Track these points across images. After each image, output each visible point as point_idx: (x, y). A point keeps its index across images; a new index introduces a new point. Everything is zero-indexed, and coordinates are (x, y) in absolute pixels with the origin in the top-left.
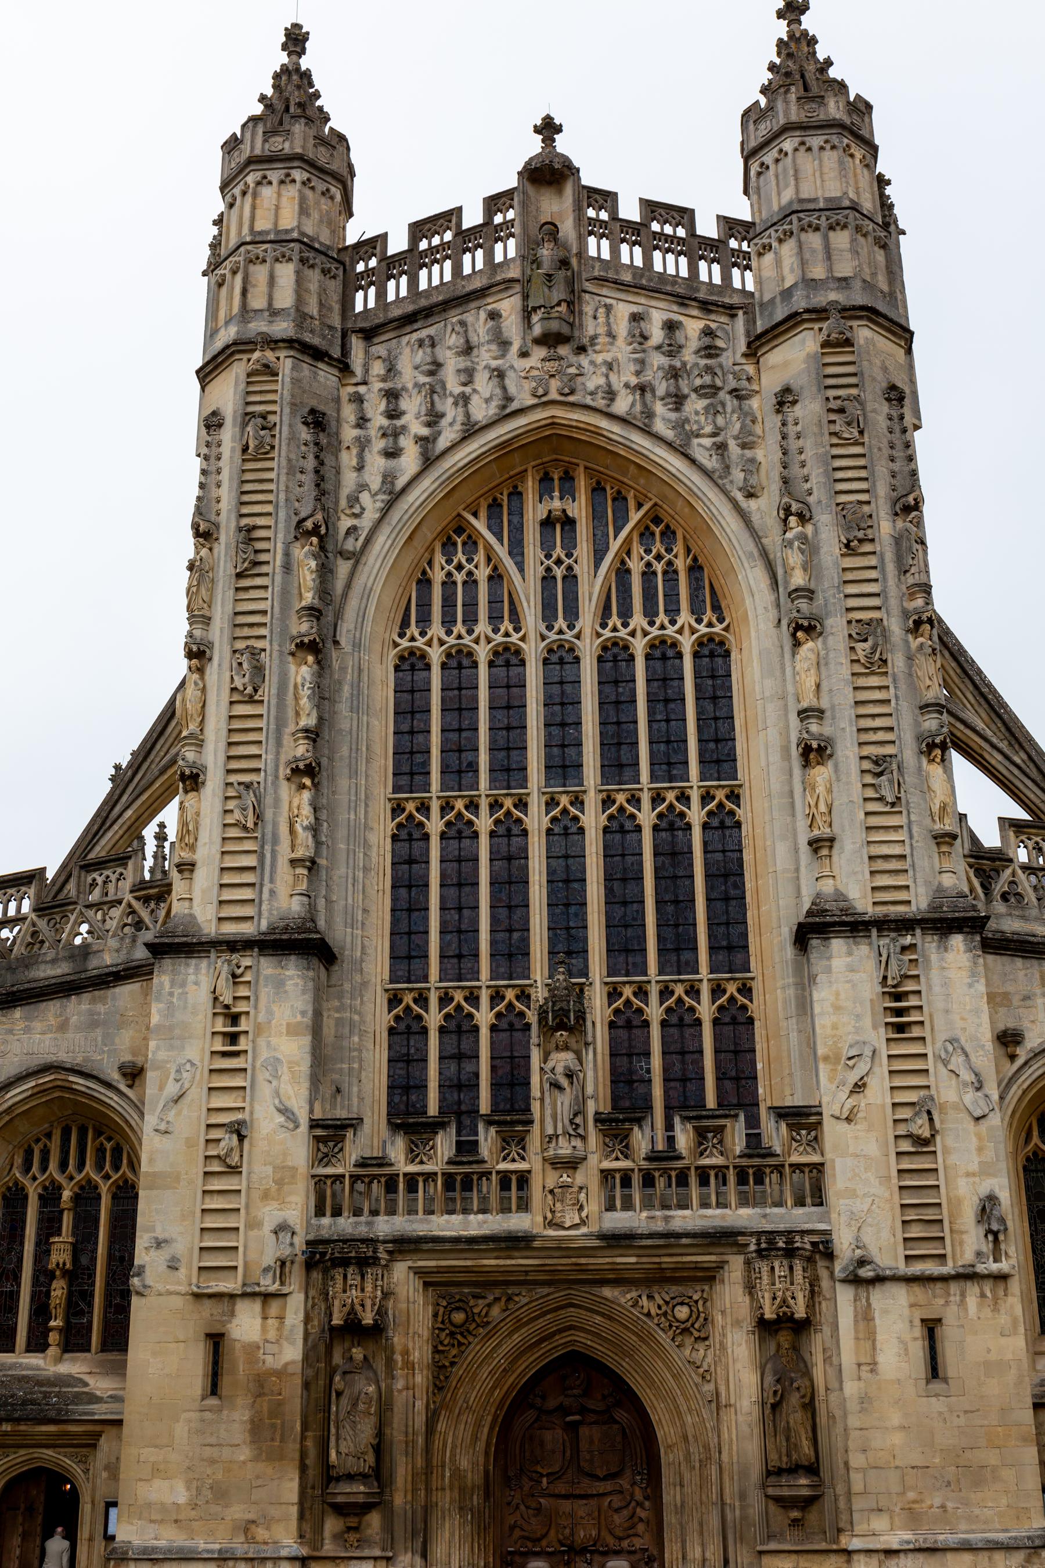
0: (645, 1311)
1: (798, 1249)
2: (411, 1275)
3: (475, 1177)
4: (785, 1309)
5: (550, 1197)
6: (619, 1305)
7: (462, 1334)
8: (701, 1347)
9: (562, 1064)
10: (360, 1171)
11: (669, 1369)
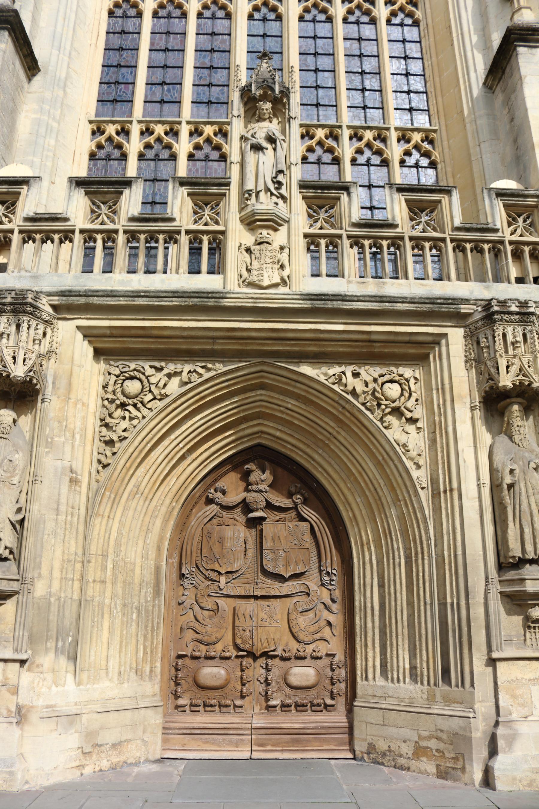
0: (350, 388)
1: (532, 314)
2: (80, 336)
3: (161, 237)
4: (520, 377)
5: (247, 256)
6: (319, 382)
7: (135, 406)
8: (411, 428)
9: (265, 130)
10: (29, 226)
11: (372, 456)
